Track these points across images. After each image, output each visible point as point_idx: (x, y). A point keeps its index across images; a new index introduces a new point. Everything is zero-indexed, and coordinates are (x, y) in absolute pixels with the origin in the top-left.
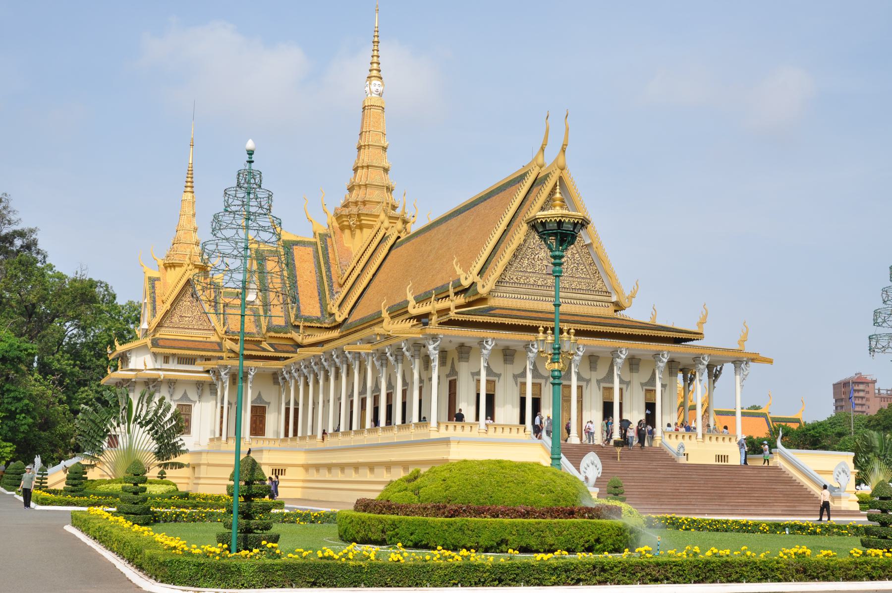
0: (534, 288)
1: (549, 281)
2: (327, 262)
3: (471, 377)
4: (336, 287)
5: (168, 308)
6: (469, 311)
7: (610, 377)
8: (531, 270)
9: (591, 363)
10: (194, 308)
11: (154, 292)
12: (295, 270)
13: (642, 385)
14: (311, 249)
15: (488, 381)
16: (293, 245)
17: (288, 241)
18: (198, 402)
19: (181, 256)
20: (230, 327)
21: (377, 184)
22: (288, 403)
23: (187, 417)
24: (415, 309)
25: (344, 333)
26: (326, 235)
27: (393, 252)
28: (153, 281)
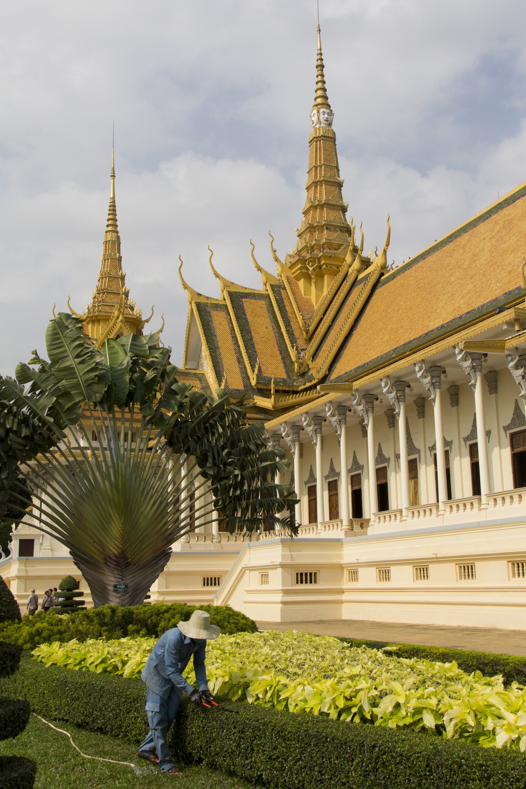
4: (301, 343)
16: (242, 297)
17: (235, 292)
19: (107, 308)
21: (336, 224)
26: (279, 286)
27: (378, 291)
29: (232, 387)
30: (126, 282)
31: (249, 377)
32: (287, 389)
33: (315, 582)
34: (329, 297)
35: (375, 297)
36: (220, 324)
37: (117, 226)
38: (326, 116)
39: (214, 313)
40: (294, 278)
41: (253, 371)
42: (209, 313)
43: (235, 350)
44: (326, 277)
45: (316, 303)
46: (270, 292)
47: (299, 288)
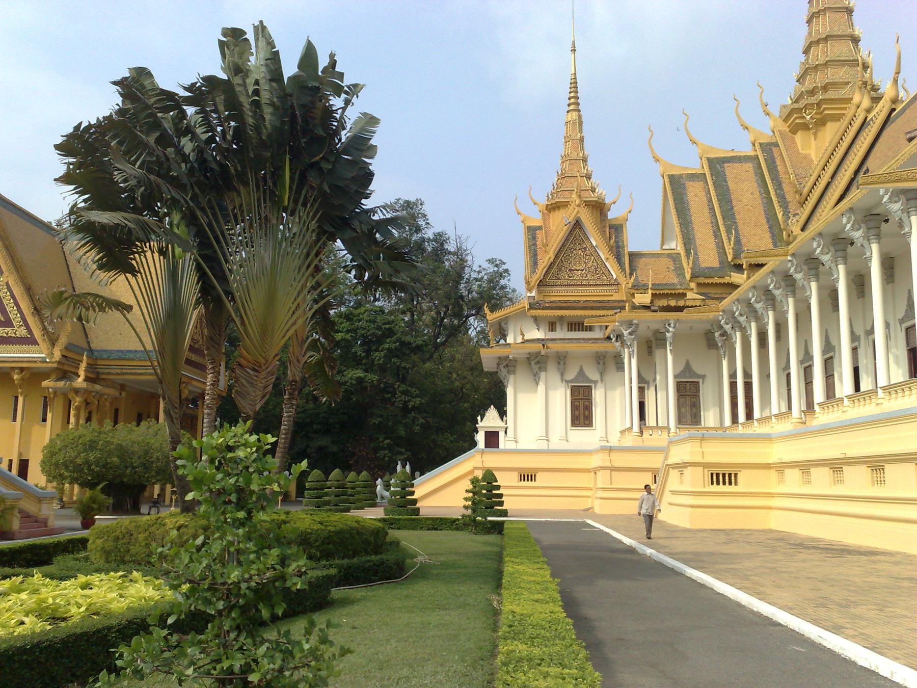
4: (792, 208)
5: (552, 260)
10: (587, 257)
11: (535, 245)
14: (750, 165)
16: (724, 162)
18: (599, 381)
19: (567, 193)
20: (640, 279)
21: (843, 59)
22: (733, 375)
23: (587, 403)
28: (532, 232)
29: (703, 265)
31: (726, 253)
33: (736, 484)
36: (695, 196)
37: (579, 104)
42: (684, 185)
43: (712, 223)
45: (816, 157)
46: (759, 153)
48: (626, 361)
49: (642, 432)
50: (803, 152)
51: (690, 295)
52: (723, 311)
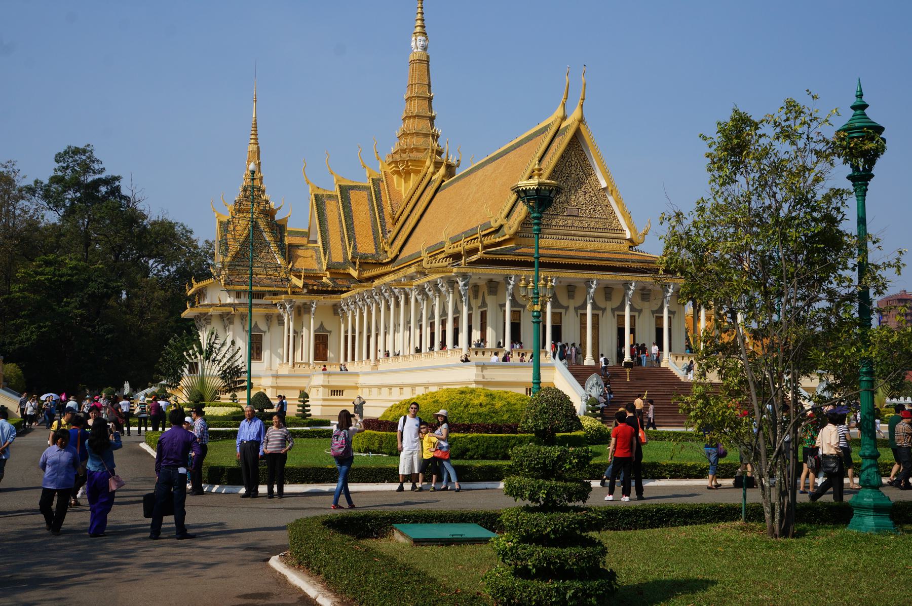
0: (556, 228)
1: (569, 221)
2: (380, 205)
3: (499, 308)
4: (389, 226)
6: (496, 251)
7: (622, 307)
8: (553, 213)
9: (606, 294)
12: (351, 212)
13: (653, 312)
14: (365, 193)
15: (512, 311)
17: (345, 186)
22: (346, 332)
23: (258, 345)
24: (449, 249)
25: (396, 268)
26: (379, 180)
27: (438, 194)
29: (334, 260)
30: (263, 181)
32: (374, 261)
34: (412, 192)
35: (435, 199)
36: (331, 211)
38: (422, 43)
39: (327, 202)
40: (391, 173)
41: (350, 247)
42: (324, 202)
44: (412, 174)
45: (405, 193)
46: (371, 185)
47: (393, 181)
48: (286, 321)
49: (294, 366)
50: (397, 189)
51: (325, 280)
52: (343, 299)
